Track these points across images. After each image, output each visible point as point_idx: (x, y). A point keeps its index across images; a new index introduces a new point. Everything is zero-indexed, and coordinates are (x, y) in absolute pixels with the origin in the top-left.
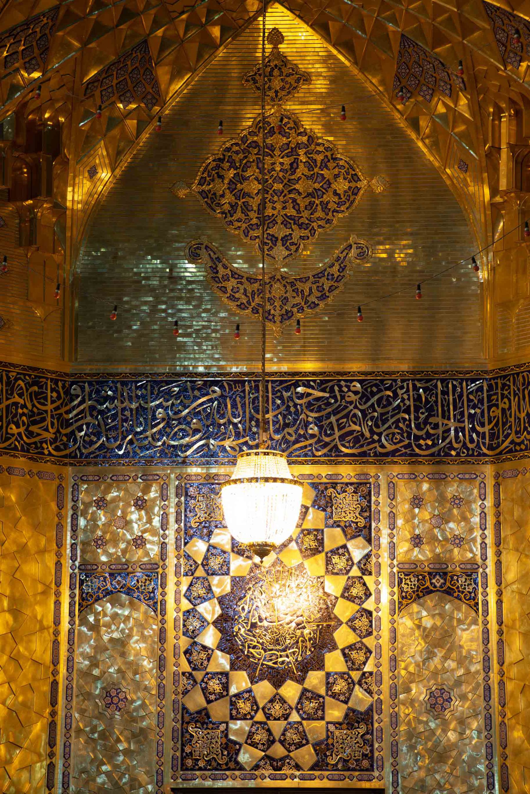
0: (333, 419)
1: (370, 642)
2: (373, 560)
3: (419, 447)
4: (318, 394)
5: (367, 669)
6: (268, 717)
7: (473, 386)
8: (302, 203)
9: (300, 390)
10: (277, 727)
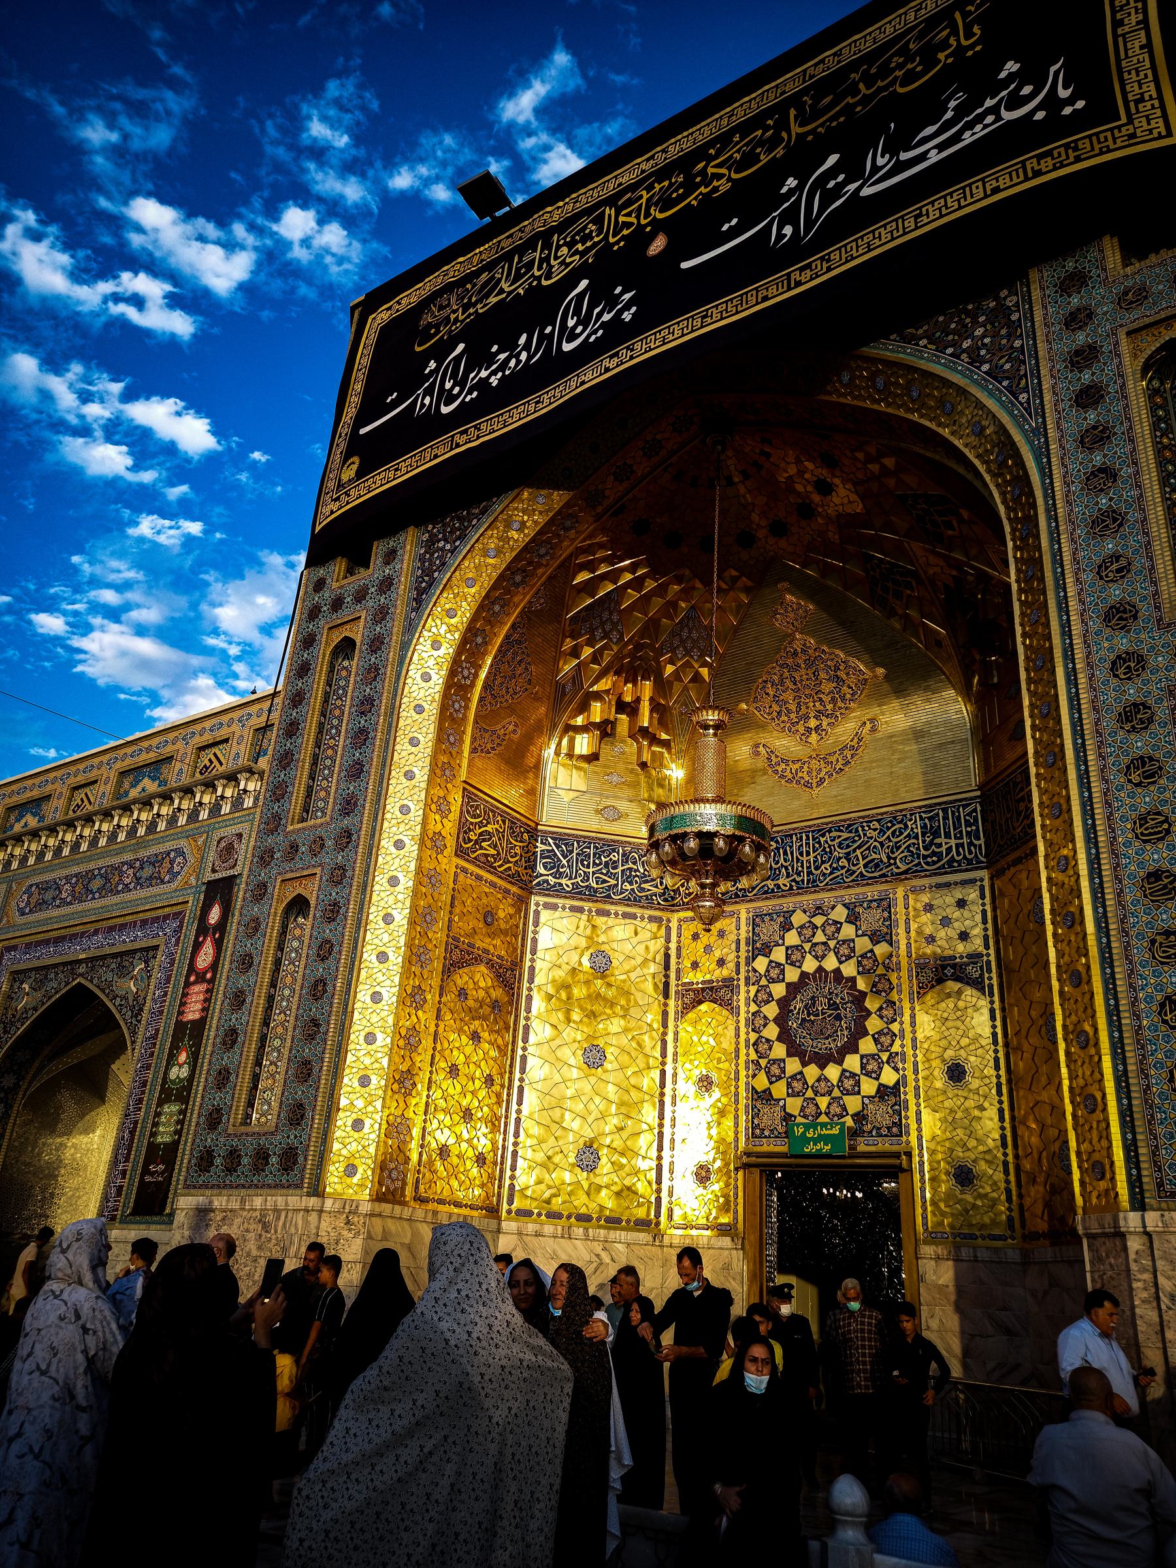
0: (858, 852)
1: (895, 1027)
2: (894, 959)
3: (927, 864)
4: (845, 835)
5: (894, 1049)
6: (816, 1093)
7: (968, 810)
8: (827, 699)
9: (834, 834)
10: (823, 1102)
